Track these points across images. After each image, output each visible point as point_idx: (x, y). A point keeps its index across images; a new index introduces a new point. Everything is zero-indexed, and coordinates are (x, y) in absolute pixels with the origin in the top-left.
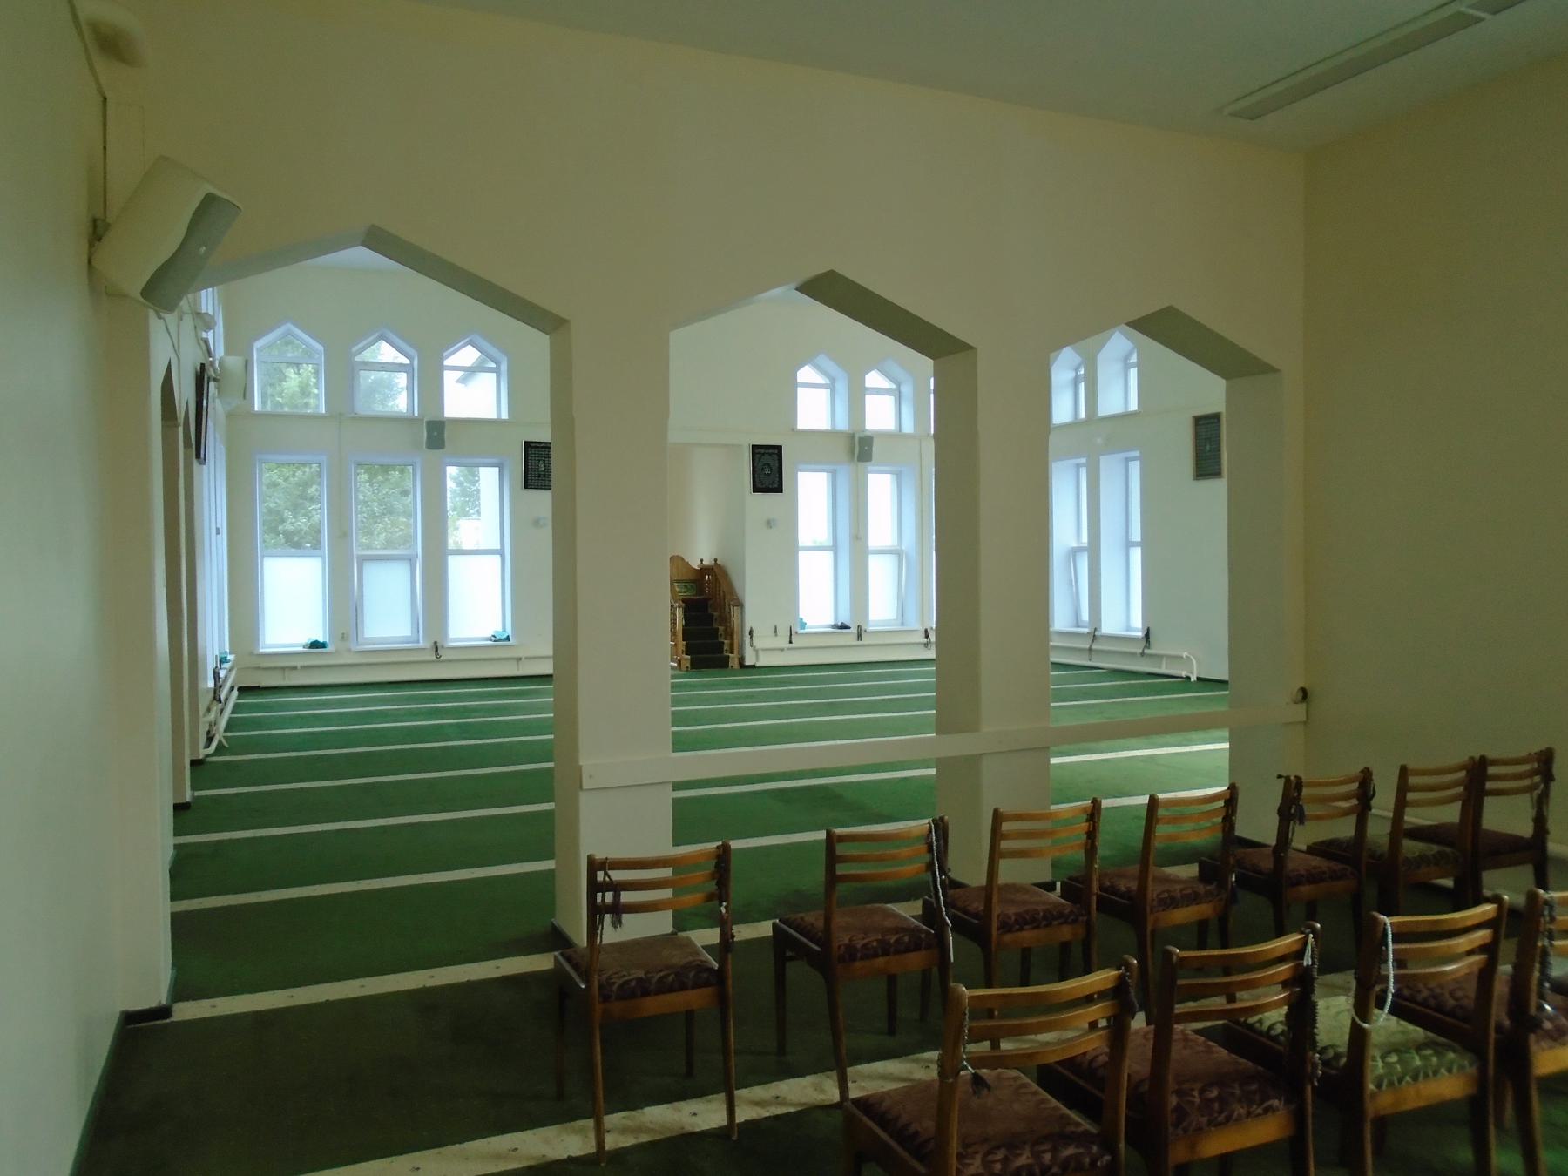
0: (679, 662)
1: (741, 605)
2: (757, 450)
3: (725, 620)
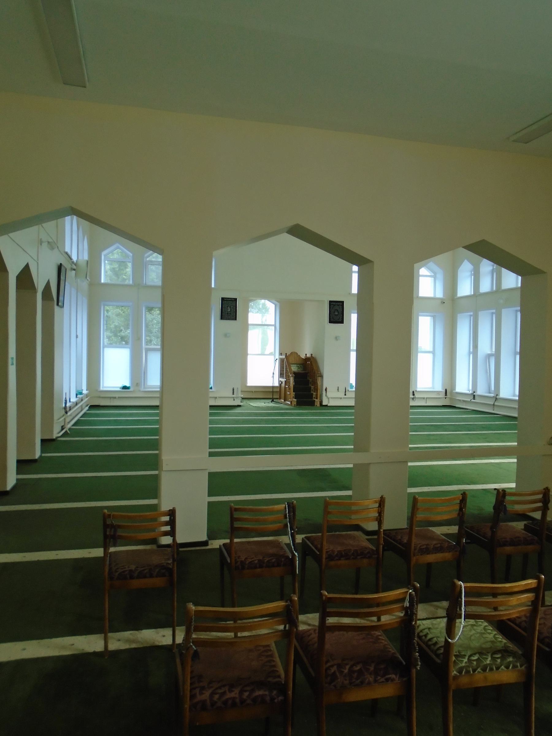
0: (291, 402)
1: (322, 376)
3: (315, 383)
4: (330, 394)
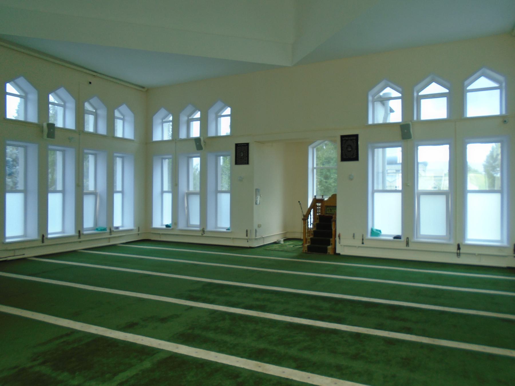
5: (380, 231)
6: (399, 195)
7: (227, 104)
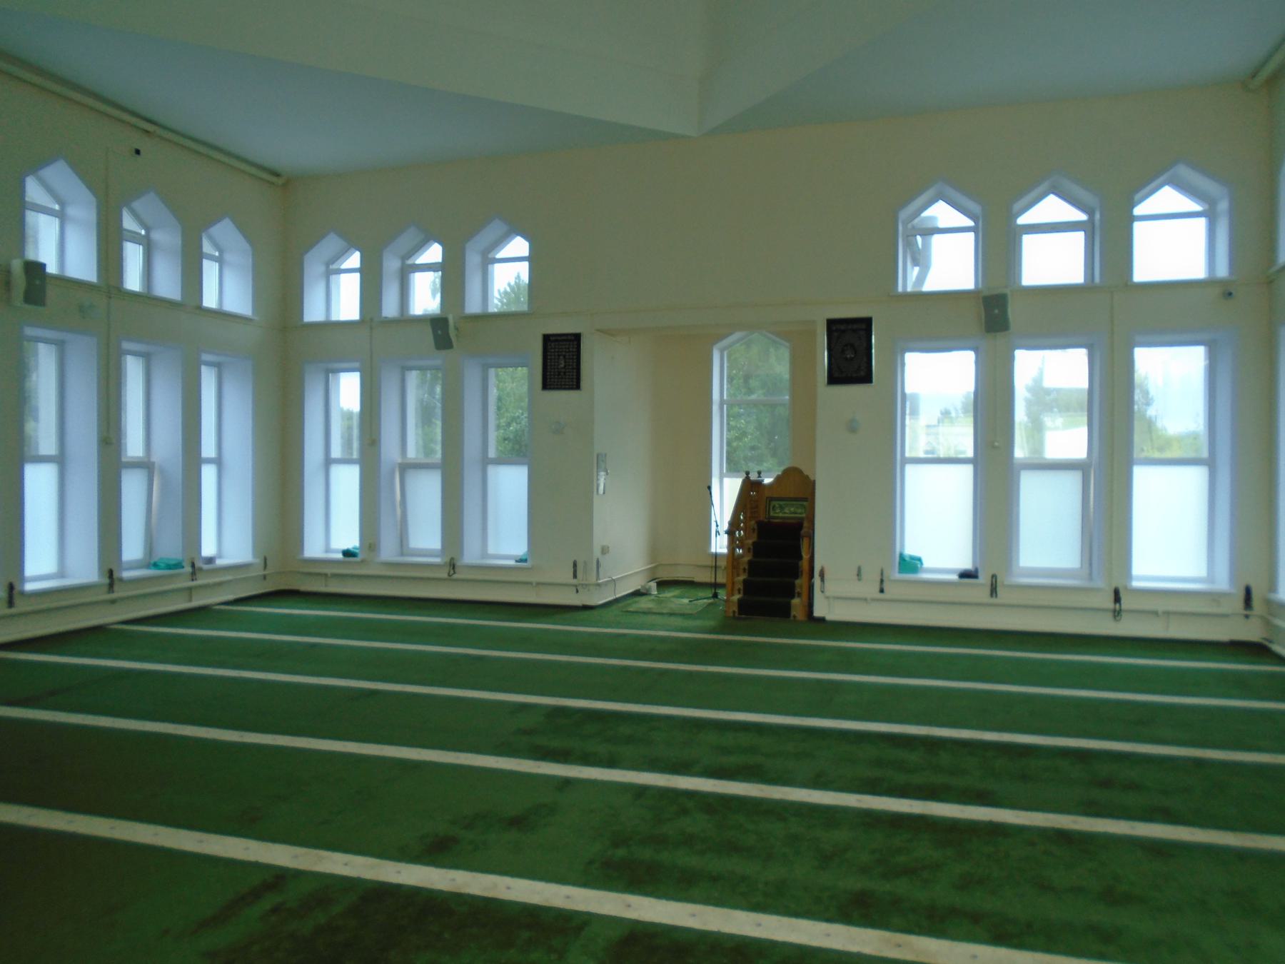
2: (835, 327)
4: (832, 587)
5: (920, 560)
6: (967, 472)
7: (516, 229)
